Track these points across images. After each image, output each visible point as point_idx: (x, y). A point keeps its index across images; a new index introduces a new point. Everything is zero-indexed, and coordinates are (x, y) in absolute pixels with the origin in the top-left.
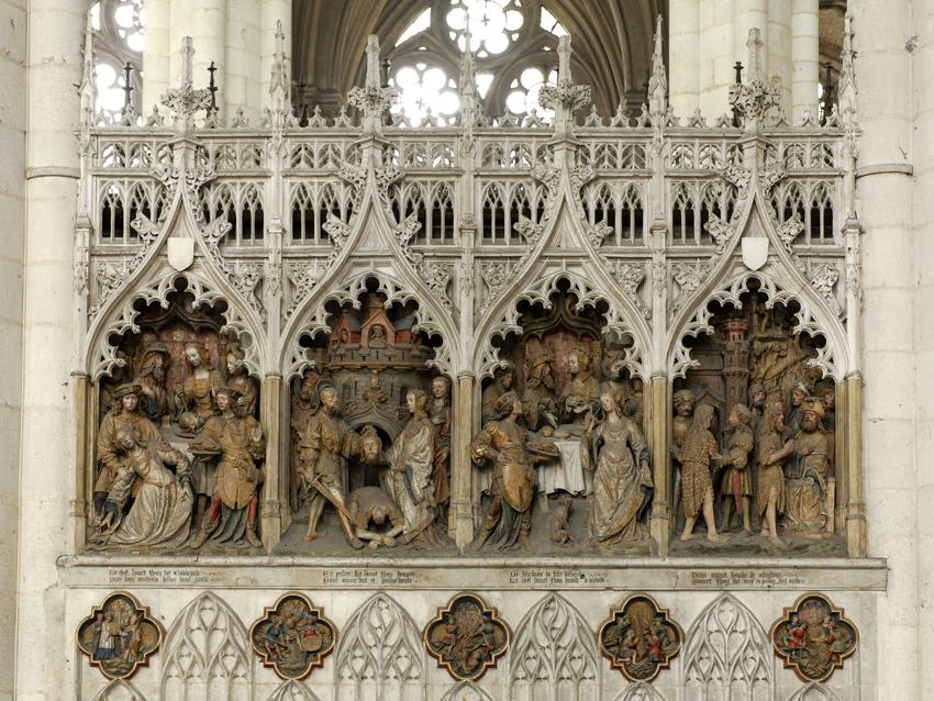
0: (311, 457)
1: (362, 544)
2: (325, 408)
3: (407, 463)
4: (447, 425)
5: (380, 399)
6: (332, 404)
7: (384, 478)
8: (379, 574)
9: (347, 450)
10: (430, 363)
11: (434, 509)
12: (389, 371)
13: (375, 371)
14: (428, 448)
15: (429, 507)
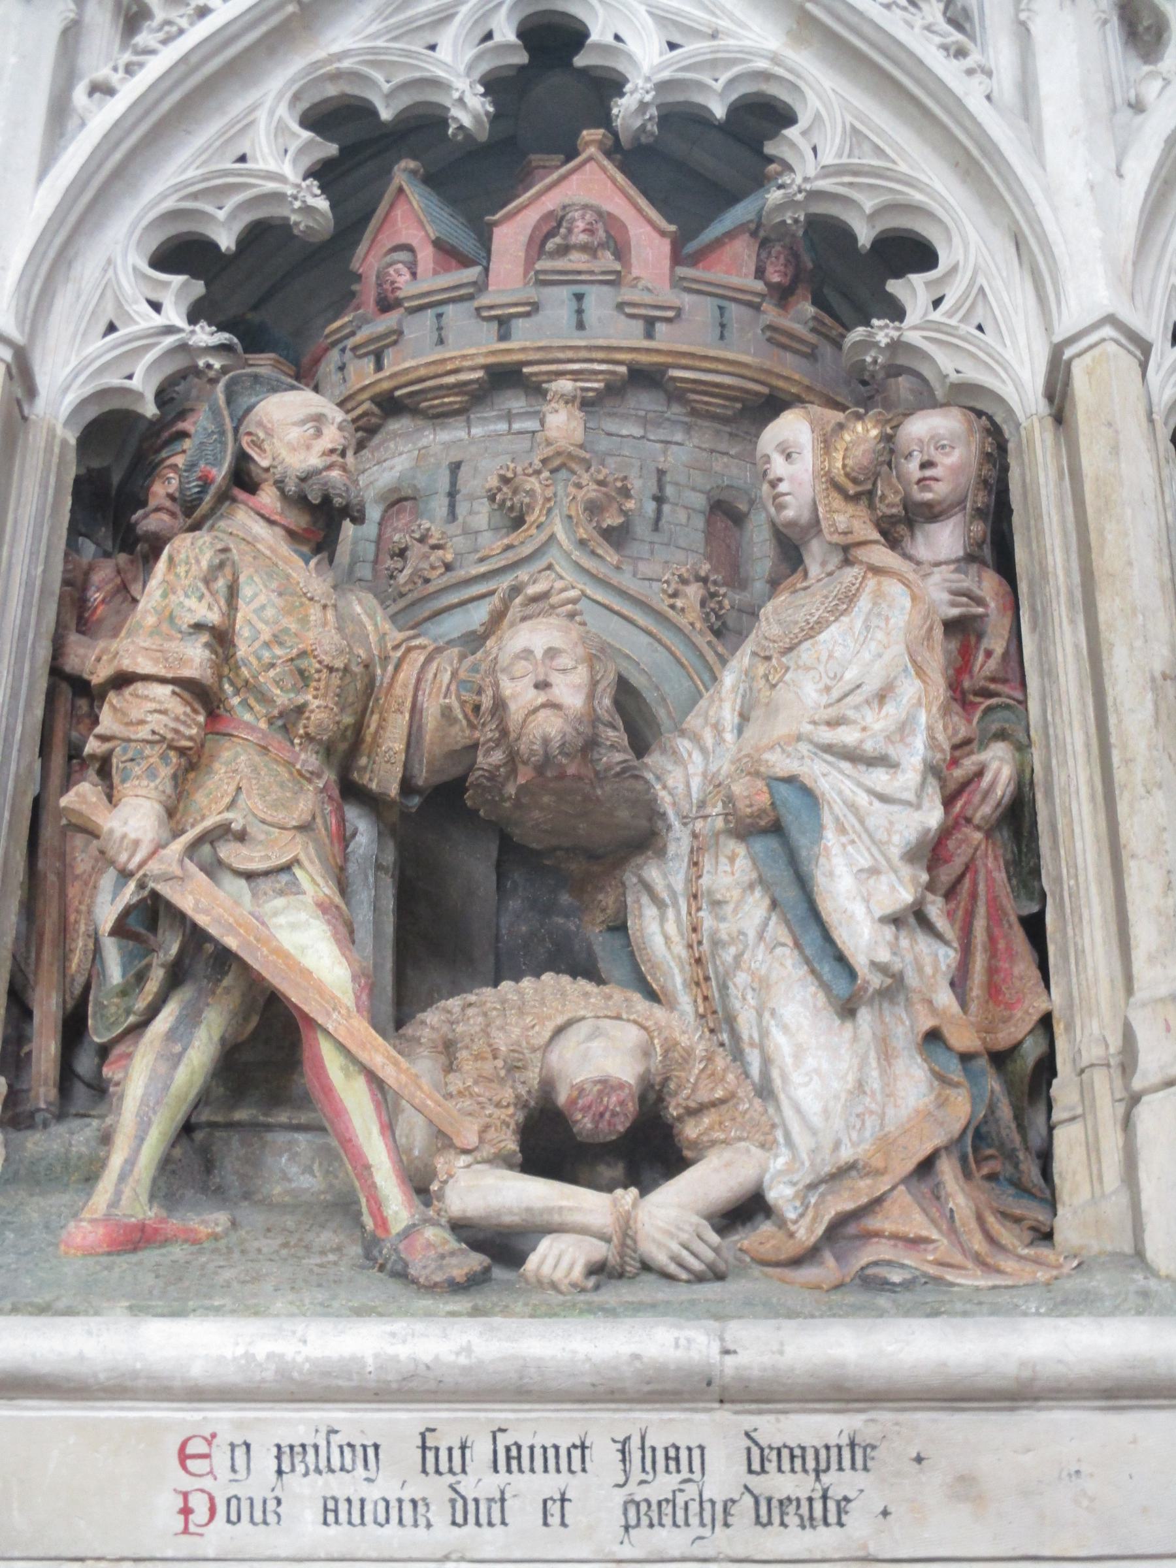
0: (158, 722)
1: (476, 1261)
2: (268, 497)
3: (781, 763)
4: (996, 642)
5: (593, 509)
6: (314, 460)
7: (619, 927)
8: (604, 1456)
9: (394, 741)
10: (883, 332)
11: (966, 1058)
12: (646, 401)
13: (565, 385)
14: (910, 688)
15: (933, 1036)
